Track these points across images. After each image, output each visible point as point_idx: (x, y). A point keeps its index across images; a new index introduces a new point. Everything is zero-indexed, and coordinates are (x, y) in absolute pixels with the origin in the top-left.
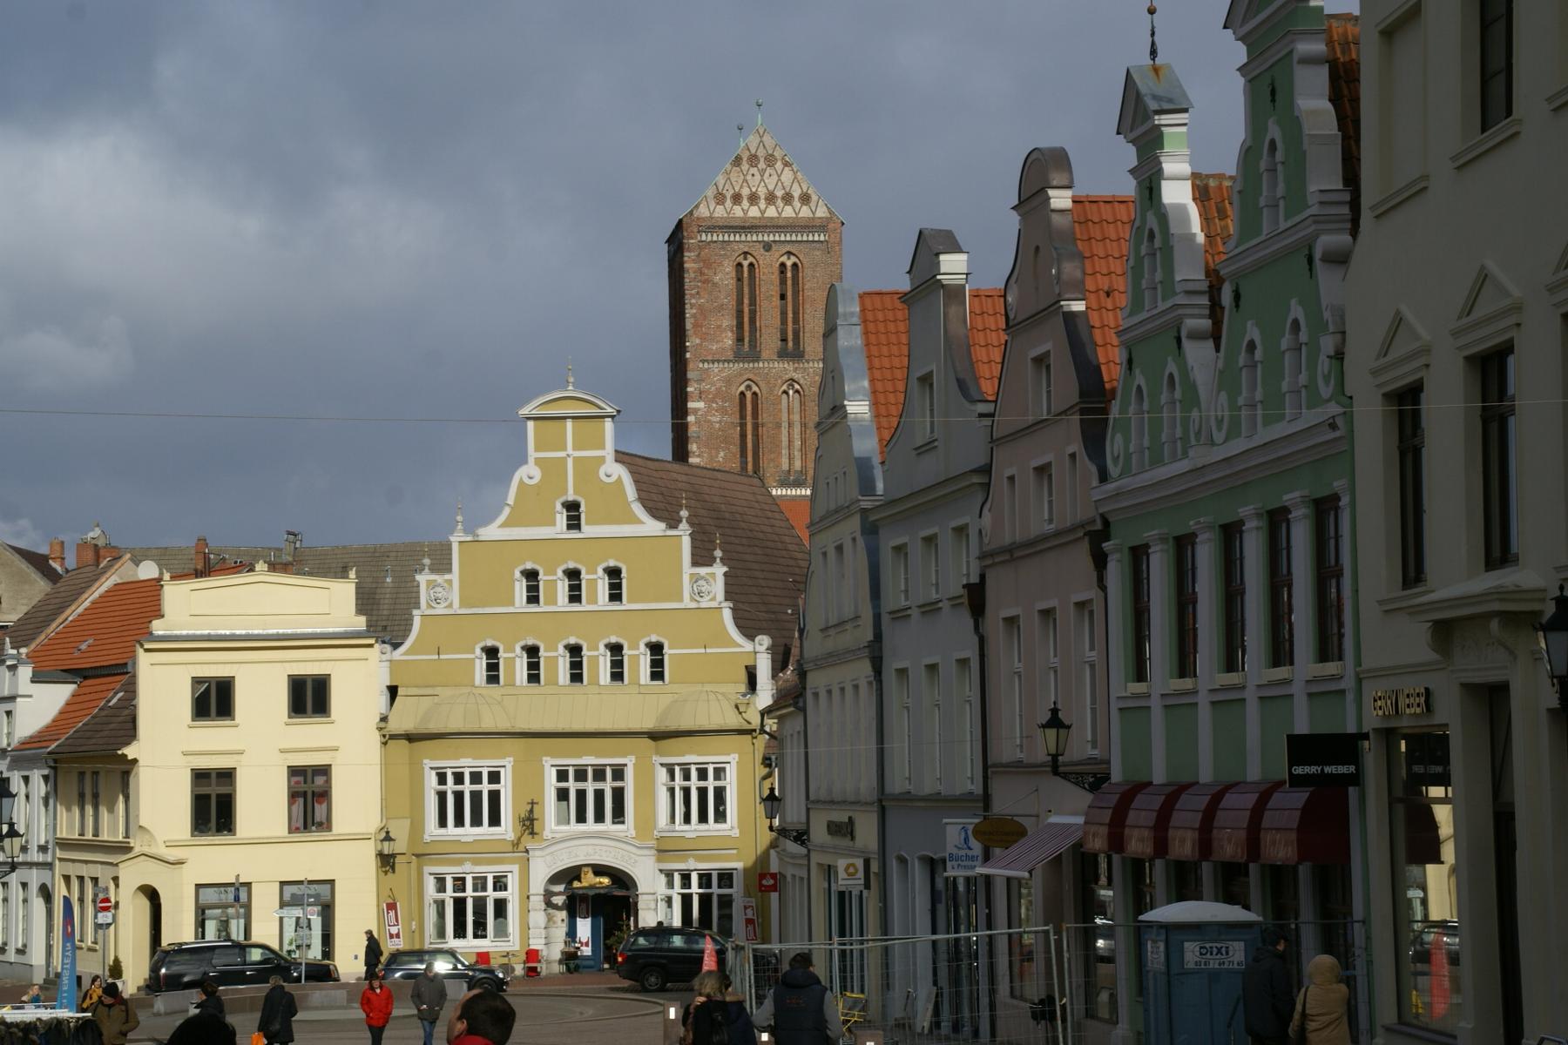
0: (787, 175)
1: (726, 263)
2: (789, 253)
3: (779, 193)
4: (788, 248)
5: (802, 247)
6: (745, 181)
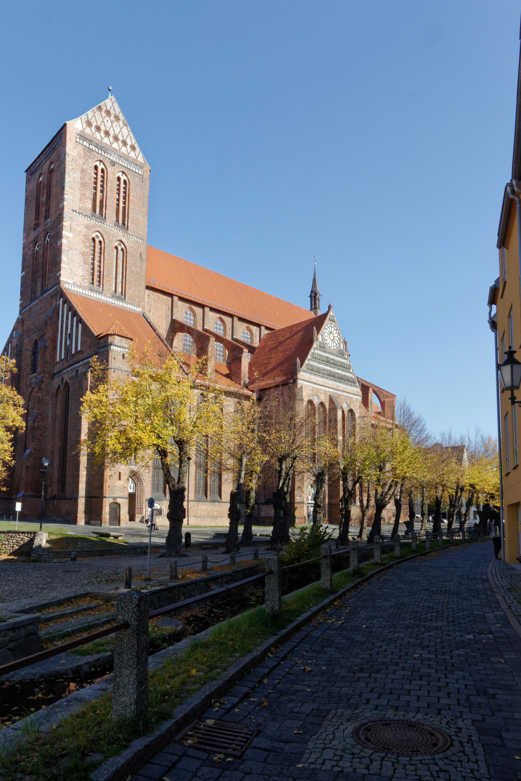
0: (125, 131)
1: (90, 161)
2: (123, 172)
3: (121, 138)
4: (123, 169)
5: (130, 172)
6: (103, 121)
